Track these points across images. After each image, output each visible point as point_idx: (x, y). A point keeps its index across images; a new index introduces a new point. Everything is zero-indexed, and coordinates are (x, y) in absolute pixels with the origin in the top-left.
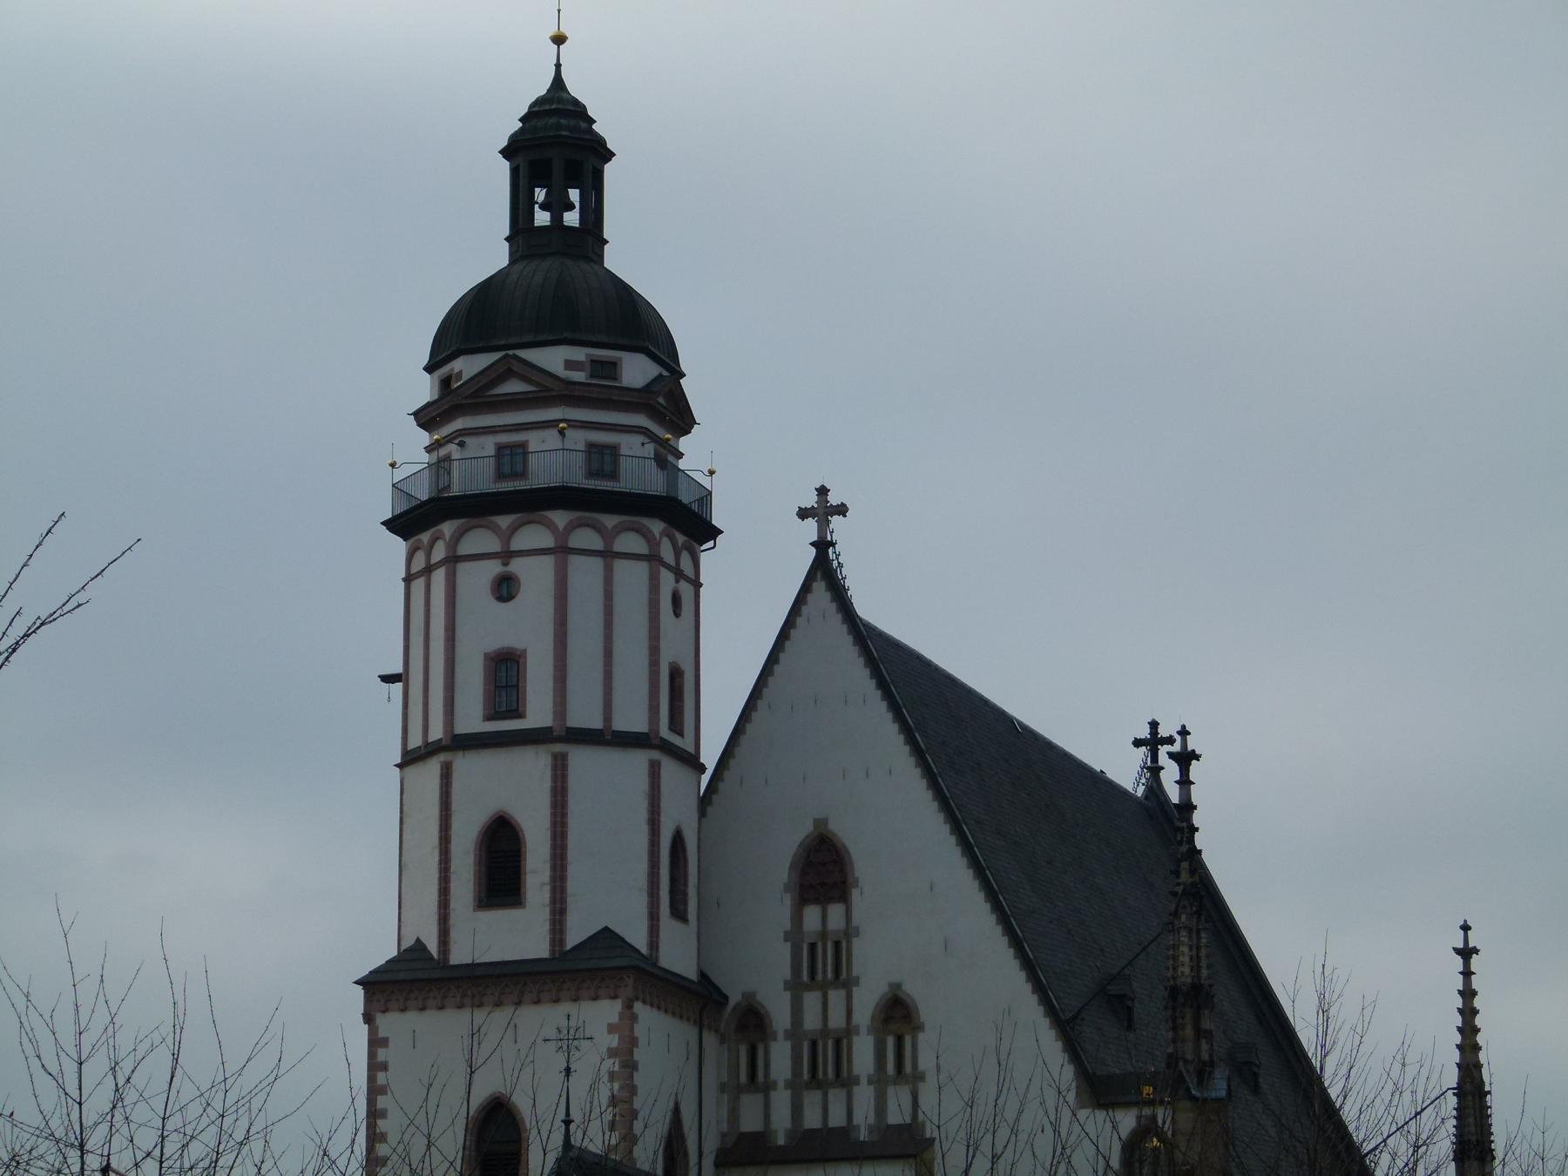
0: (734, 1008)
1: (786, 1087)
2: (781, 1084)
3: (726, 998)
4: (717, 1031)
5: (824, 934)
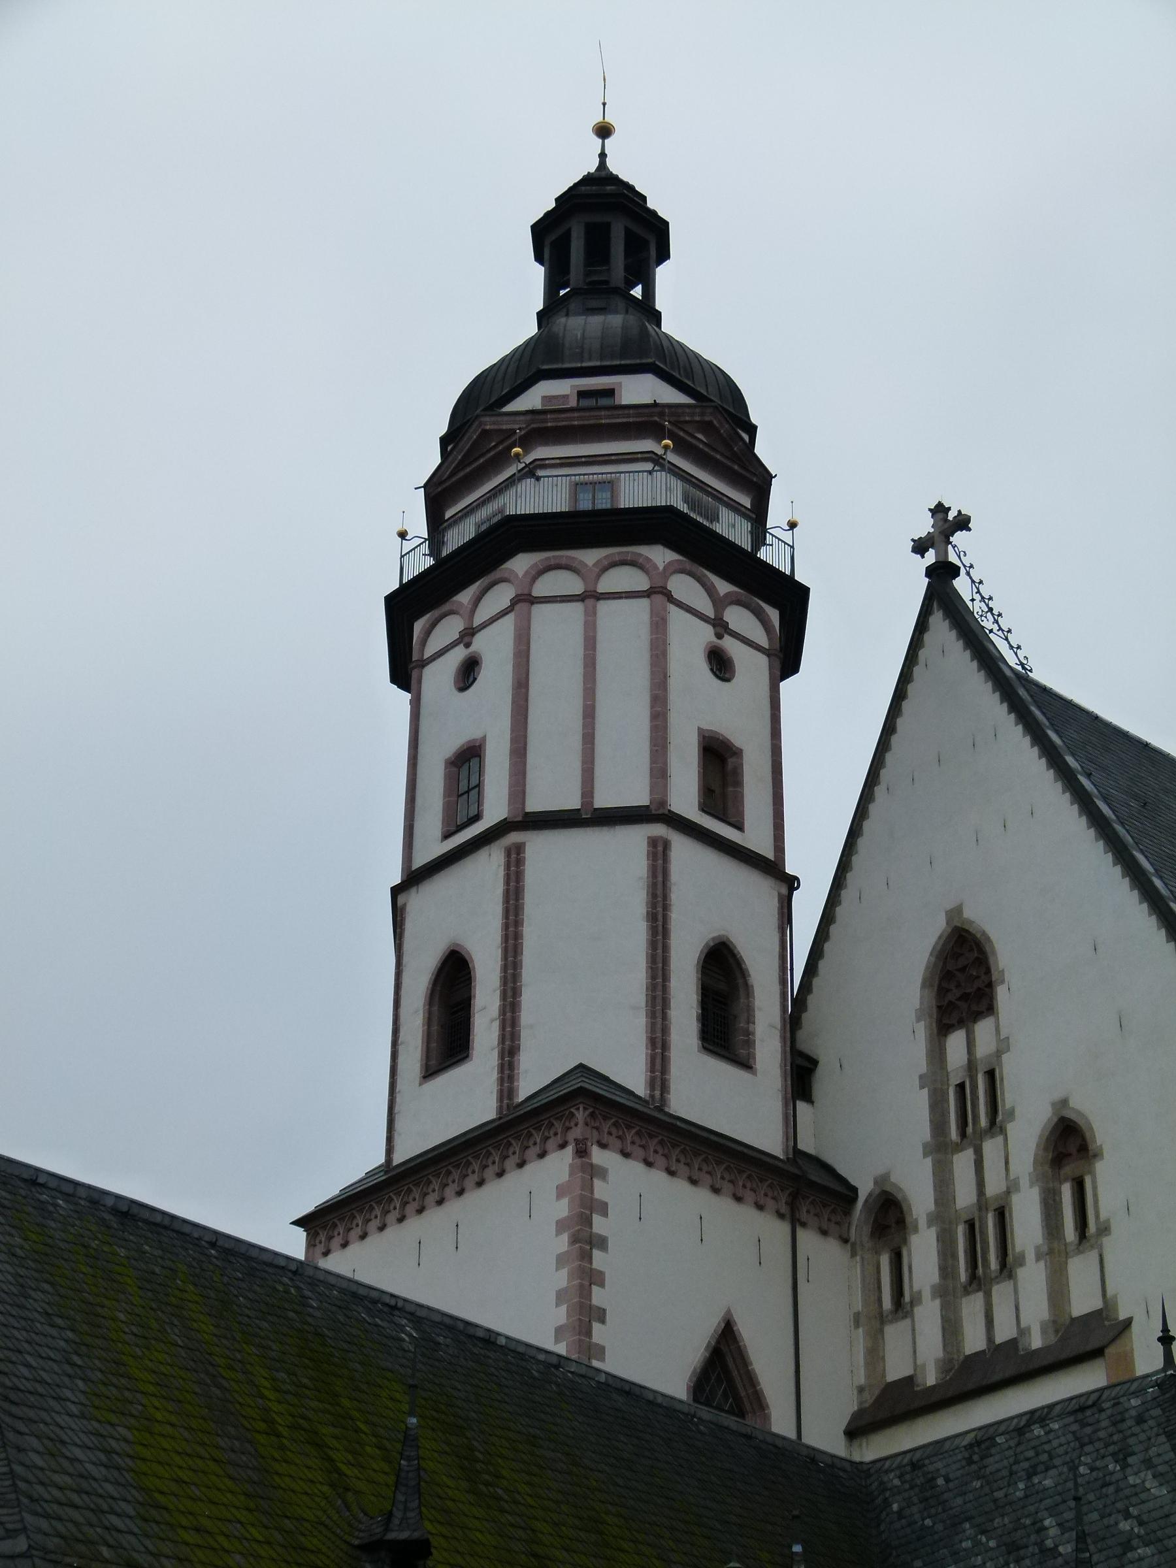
0: (866, 1201)
1: (933, 1297)
2: (927, 1294)
3: (854, 1190)
4: (845, 1241)
5: (971, 1066)
